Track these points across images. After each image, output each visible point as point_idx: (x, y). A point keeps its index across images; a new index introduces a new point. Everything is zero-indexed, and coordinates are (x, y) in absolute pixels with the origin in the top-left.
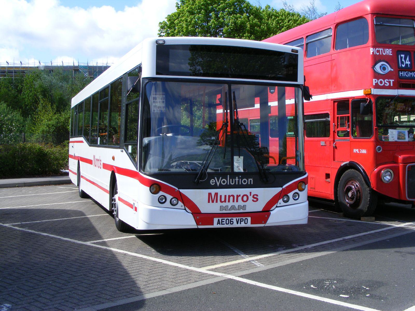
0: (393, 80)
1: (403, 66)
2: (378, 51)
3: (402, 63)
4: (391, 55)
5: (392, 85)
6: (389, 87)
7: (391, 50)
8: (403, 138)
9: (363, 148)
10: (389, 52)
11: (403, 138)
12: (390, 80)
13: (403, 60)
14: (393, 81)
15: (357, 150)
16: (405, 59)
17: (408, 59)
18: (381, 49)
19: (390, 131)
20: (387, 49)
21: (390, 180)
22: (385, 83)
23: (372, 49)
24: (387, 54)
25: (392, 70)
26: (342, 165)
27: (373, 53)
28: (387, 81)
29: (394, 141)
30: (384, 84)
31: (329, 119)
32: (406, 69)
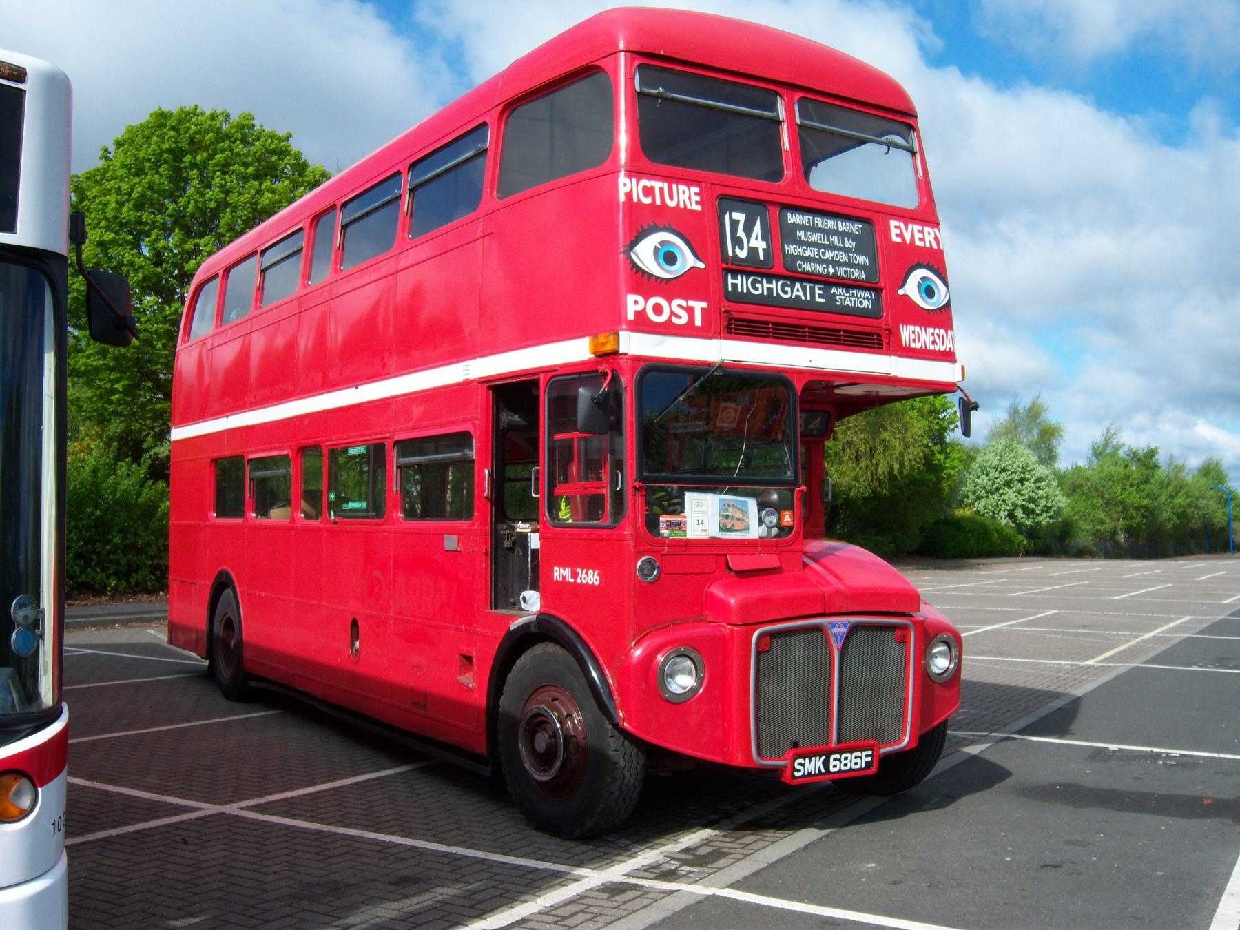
0: (705, 305)
1: (742, 254)
2: (648, 192)
3: (737, 242)
4: (699, 208)
5: (698, 322)
6: (688, 331)
8: (739, 525)
9: (587, 566)
11: (739, 525)
12: (691, 303)
14: (702, 309)
15: (567, 572)
16: (748, 230)
17: (757, 229)
19: (692, 499)
20: (682, 187)
21: (693, 691)
22: (672, 313)
23: (627, 181)
25: (701, 265)
26: (512, 627)
27: (629, 195)
28: (680, 306)
30: (670, 318)
31: (473, 454)
32: (751, 268)
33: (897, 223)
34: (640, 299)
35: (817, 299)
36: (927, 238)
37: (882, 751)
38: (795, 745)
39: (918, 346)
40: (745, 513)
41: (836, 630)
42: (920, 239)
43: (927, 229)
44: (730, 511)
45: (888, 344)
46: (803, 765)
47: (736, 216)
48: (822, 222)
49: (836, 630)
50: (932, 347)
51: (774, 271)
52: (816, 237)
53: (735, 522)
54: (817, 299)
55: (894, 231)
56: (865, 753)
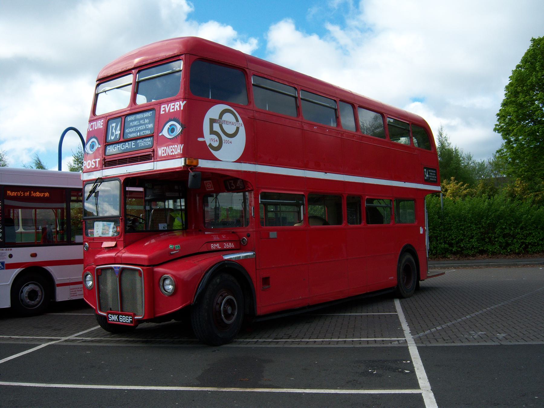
6: (95, 169)
13: (114, 131)
16: (116, 130)
36: (176, 106)
38: (111, 310)
39: (165, 155)
43: (176, 103)
45: (153, 156)
50: (171, 154)
55: (162, 109)
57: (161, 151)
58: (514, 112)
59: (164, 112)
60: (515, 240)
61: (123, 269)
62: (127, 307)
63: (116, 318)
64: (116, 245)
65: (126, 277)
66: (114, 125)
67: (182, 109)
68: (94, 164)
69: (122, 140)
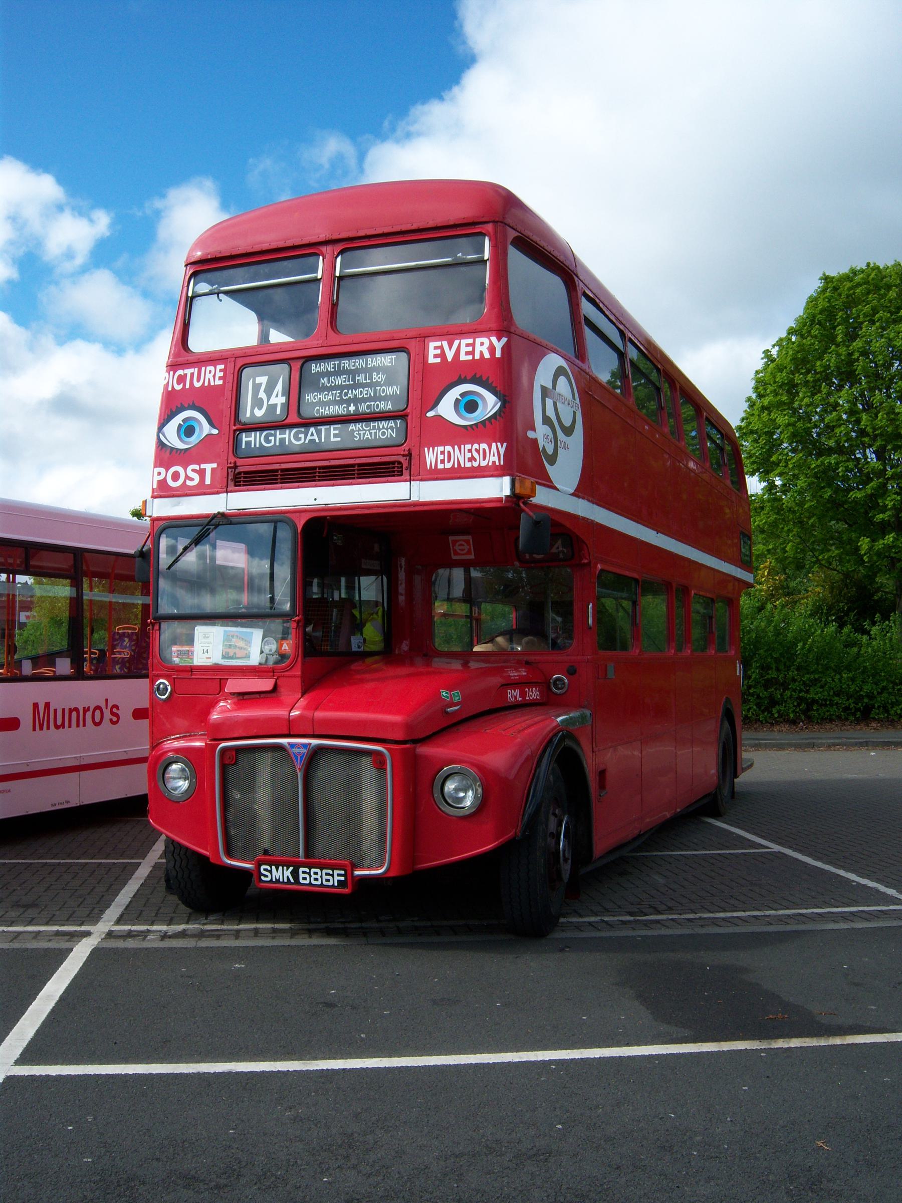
0: (215, 465)
3: (258, 403)
4: (221, 382)
5: (208, 481)
6: (201, 490)
7: (222, 367)
8: (240, 653)
10: (214, 376)
12: (203, 466)
13: (262, 395)
14: (213, 470)
16: (269, 391)
18: (192, 370)
20: (209, 368)
22: (187, 477)
24: (206, 384)
25: (215, 432)
28: (193, 470)
29: (208, 663)
30: (185, 481)
33: (438, 344)
34: (163, 470)
35: (332, 439)
36: (478, 348)
37: (357, 873)
39: (448, 466)
40: (249, 643)
41: (295, 750)
42: (467, 353)
43: (478, 341)
44: (234, 641)
45: (409, 467)
46: (270, 872)
47: (259, 380)
48: (347, 363)
49: (295, 750)
50: (468, 465)
51: (288, 421)
52: (339, 380)
53: (237, 651)
54: (332, 439)
56: (336, 872)
57: (432, 457)
58: (789, 425)
59: (438, 360)
60: (788, 693)
61: (320, 749)
62: (324, 845)
63: (288, 873)
64: (275, 688)
65: (325, 770)
66: (263, 380)
67: (498, 354)
68: (197, 478)
69: (293, 418)
